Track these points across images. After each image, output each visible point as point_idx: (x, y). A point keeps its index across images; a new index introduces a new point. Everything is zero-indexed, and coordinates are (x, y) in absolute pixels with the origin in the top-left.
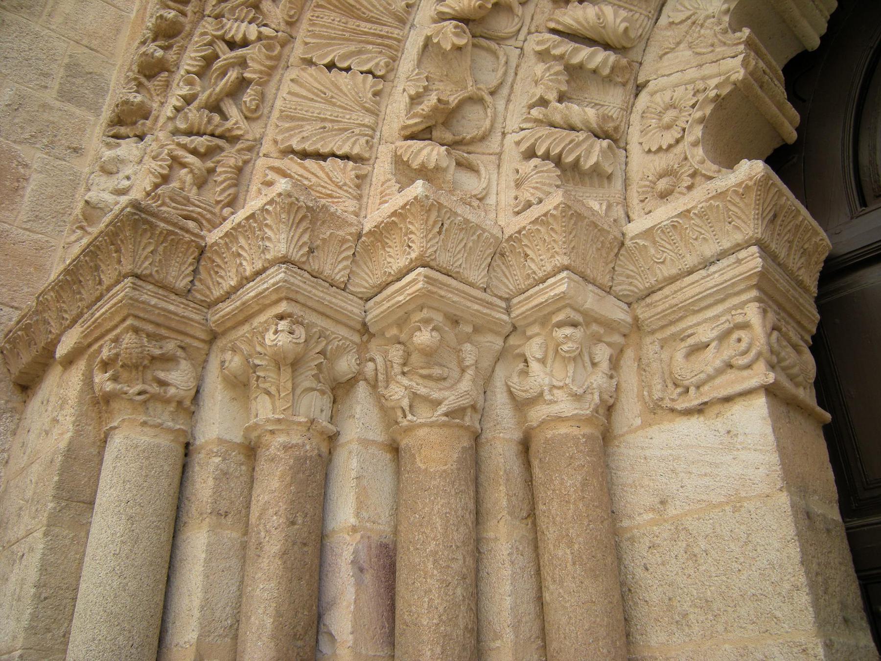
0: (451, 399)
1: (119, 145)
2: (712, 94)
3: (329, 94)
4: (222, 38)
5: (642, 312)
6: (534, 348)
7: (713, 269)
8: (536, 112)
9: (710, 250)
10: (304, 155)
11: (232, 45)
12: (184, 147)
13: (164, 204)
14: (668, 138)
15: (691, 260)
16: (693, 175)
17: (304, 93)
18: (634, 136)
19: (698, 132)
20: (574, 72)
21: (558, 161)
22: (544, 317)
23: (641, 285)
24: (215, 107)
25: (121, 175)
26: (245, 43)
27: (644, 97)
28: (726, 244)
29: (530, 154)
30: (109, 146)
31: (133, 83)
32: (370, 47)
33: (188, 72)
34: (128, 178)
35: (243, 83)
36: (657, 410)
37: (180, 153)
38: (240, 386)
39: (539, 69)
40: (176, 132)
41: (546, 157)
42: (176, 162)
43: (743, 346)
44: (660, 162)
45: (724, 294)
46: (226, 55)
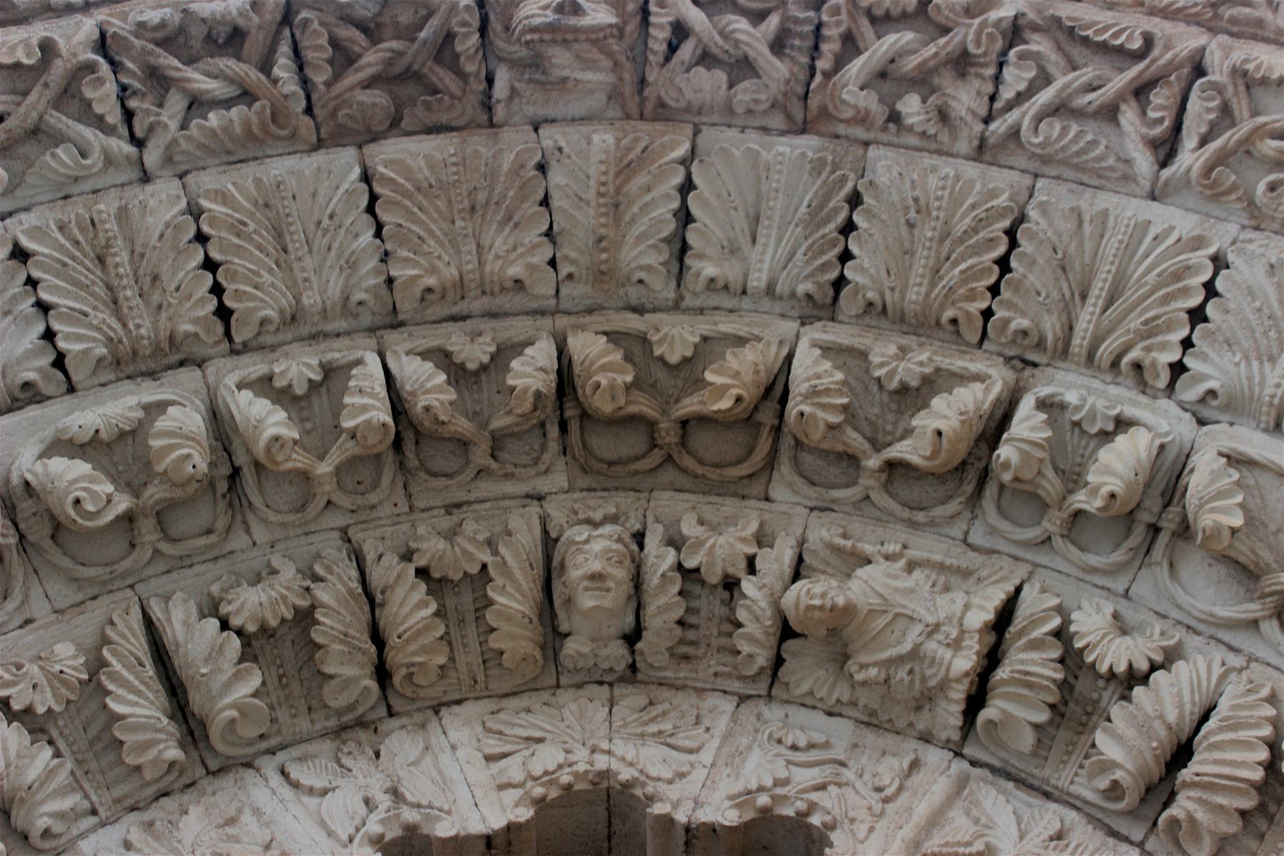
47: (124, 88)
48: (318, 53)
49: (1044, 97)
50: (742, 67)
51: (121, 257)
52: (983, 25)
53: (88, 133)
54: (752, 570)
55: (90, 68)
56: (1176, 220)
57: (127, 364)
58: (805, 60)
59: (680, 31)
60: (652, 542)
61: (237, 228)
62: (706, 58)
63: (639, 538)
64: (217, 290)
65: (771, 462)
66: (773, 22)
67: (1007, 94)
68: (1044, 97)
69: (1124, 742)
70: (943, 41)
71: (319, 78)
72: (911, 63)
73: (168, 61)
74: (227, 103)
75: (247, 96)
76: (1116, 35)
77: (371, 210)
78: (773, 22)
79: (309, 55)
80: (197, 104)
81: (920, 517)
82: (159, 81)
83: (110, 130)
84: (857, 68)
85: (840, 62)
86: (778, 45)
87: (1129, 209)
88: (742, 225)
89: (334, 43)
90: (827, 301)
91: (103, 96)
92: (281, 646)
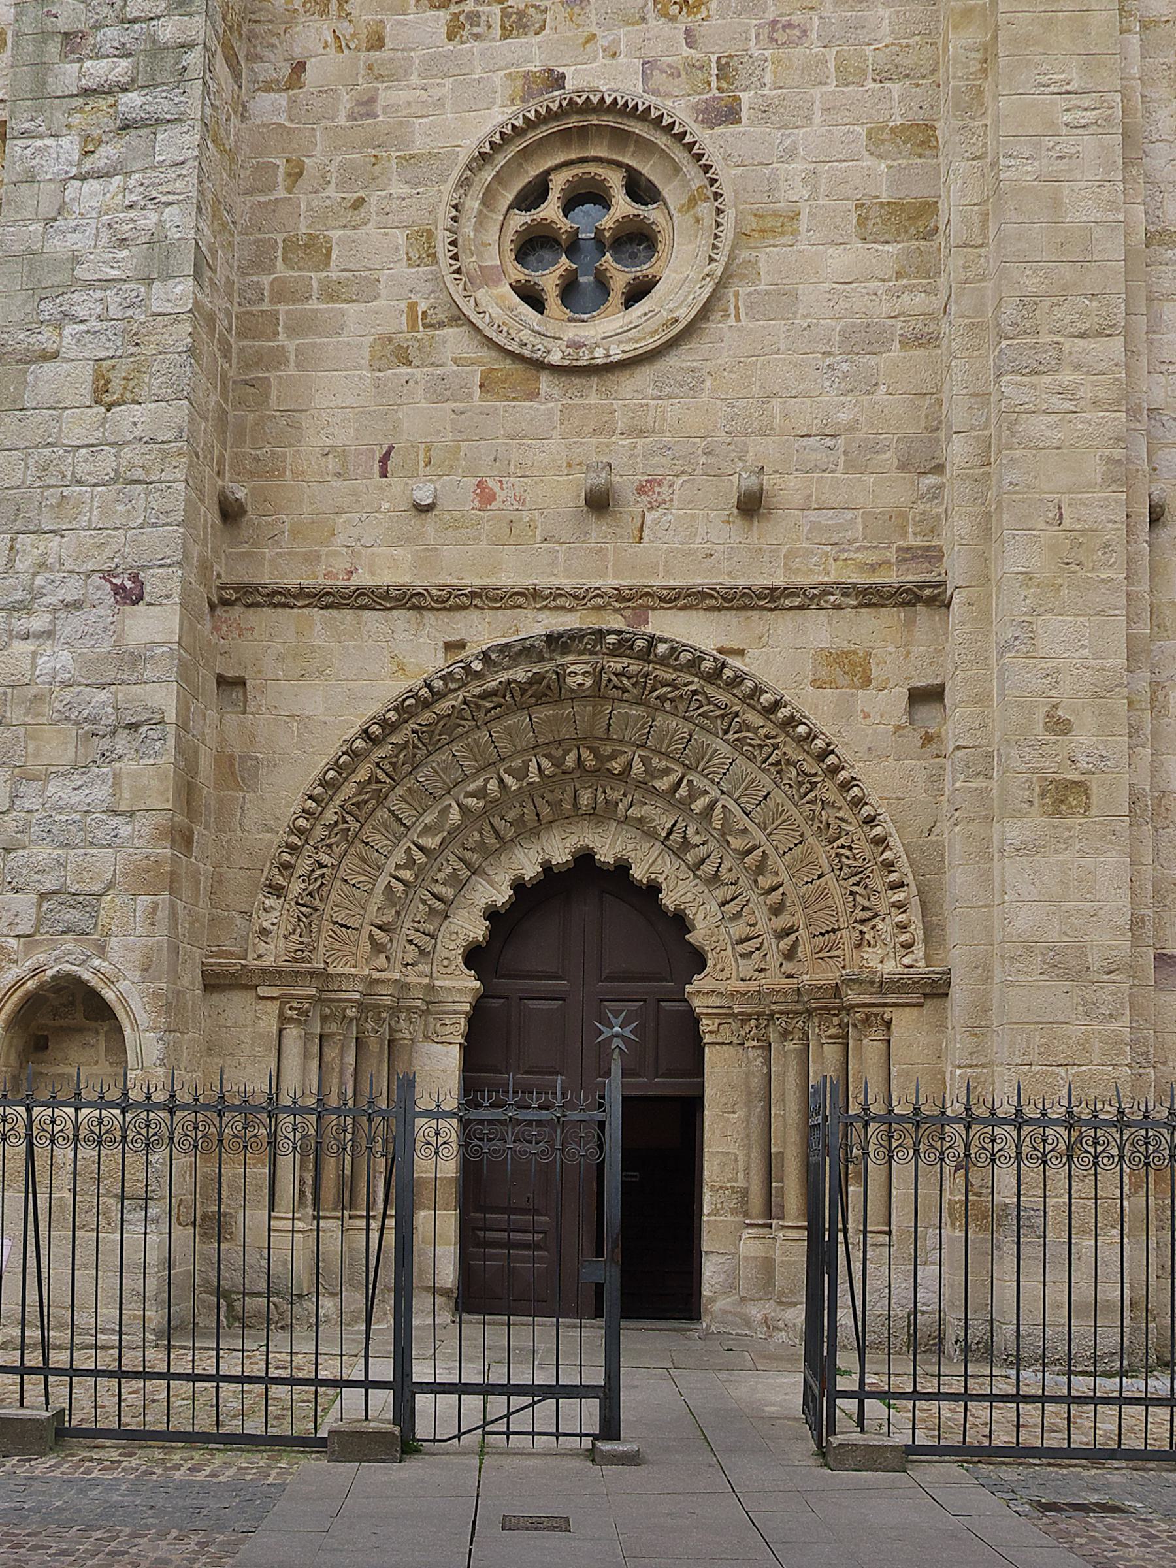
0: (382, 1030)
5: (432, 1007)
6: (403, 1016)
8: (416, 925)
10: (342, 925)
11: (321, 866)
18: (440, 938)
20: (432, 911)
22: (408, 1009)
23: (433, 999)
25: (271, 915)
27: (447, 922)
29: (410, 942)
35: (323, 884)
36: (426, 1037)
38: (324, 1019)
39: (421, 906)
40: (297, 903)
41: (416, 945)
42: (300, 920)
44: (446, 954)
46: (319, 872)
48: (517, 694)
49: (700, 711)
51: (475, 749)
53: (463, 722)
56: (725, 749)
57: (480, 770)
59: (610, 680)
61: (500, 737)
62: (615, 687)
68: (700, 711)
69: (690, 857)
72: (670, 696)
73: (481, 702)
74: (495, 708)
82: (478, 707)
85: (651, 692)
87: (717, 744)
90: (643, 746)
91: (468, 715)
92: (521, 820)
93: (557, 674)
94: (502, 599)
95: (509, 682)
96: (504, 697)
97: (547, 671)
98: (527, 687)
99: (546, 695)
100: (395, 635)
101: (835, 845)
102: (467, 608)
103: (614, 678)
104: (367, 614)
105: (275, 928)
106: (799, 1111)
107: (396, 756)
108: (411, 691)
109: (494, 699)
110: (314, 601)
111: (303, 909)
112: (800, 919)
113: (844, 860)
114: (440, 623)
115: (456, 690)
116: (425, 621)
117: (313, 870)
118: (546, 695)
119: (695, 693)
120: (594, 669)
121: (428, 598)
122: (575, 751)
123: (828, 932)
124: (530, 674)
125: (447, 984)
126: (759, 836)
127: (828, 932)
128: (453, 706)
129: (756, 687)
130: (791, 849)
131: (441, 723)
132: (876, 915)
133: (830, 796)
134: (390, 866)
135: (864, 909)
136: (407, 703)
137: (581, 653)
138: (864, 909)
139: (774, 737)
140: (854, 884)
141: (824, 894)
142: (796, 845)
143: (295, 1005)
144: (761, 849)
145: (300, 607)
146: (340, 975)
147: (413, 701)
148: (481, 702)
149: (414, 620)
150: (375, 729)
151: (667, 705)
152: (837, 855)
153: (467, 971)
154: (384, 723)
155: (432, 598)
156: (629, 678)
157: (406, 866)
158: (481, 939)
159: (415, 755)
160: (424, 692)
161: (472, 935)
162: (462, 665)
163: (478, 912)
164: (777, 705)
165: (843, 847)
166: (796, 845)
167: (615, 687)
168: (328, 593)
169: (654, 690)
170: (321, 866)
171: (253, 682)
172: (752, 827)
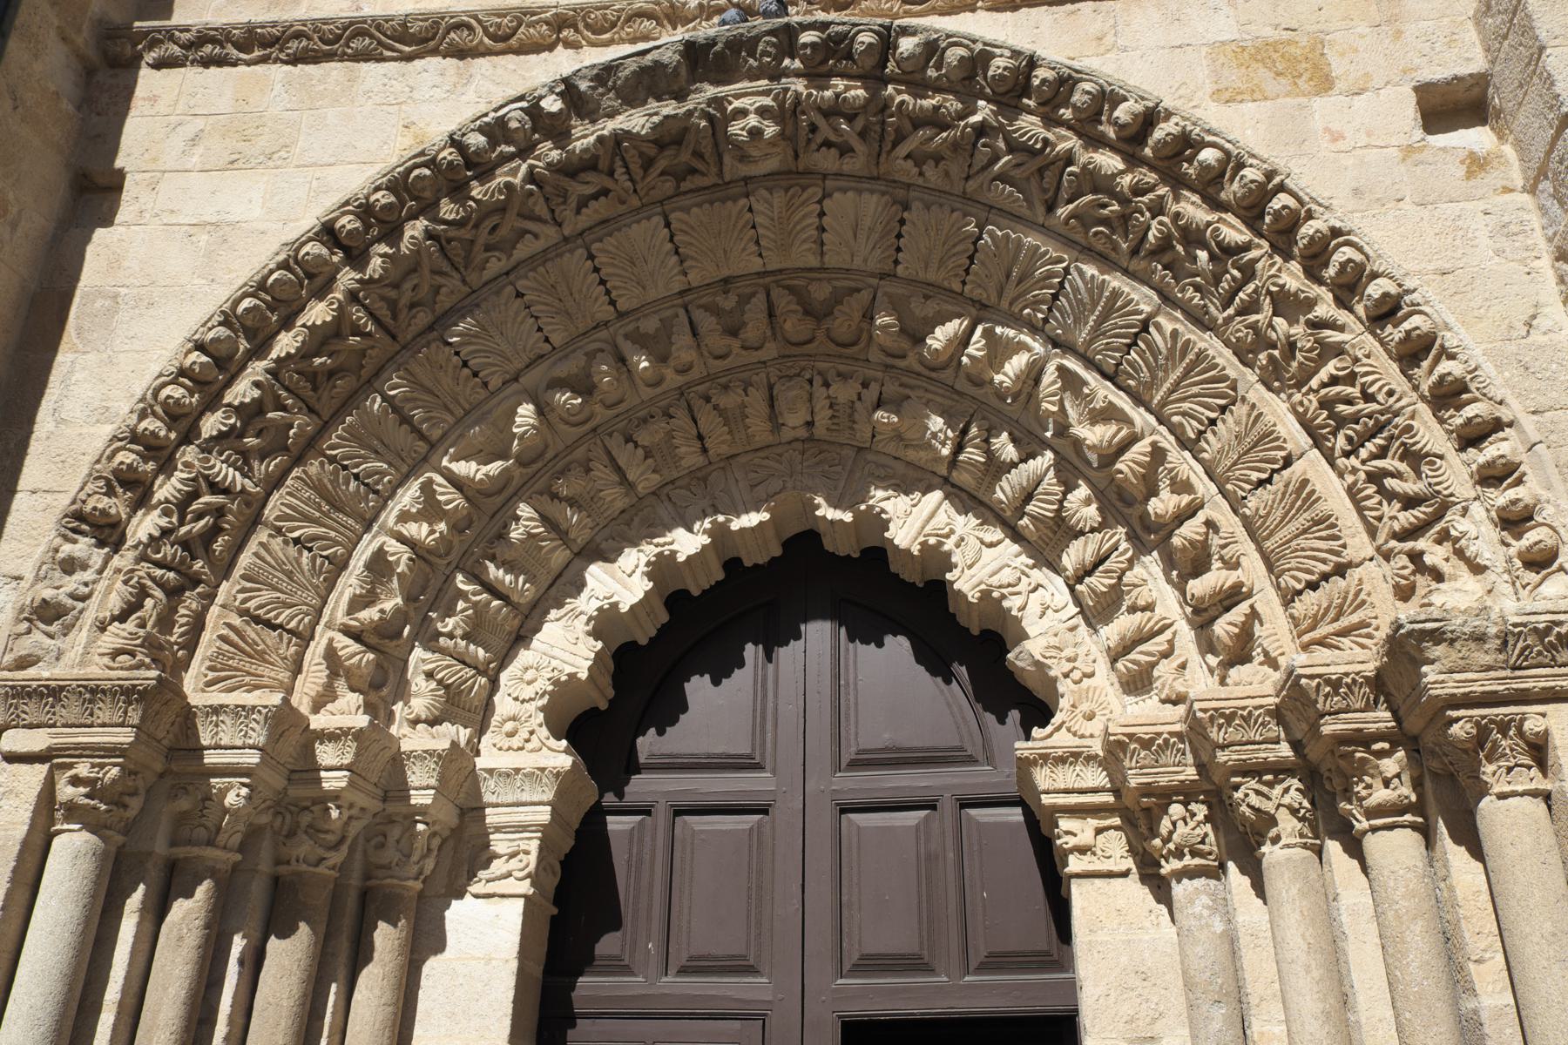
1: (75, 542)
2: (564, 678)
3: (289, 567)
4: (206, 477)
7: (521, 809)
9: (525, 797)
10: (257, 620)
11: (215, 488)
12: (153, 579)
13: (141, 646)
14: (528, 692)
15: (510, 799)
16: (532, 733)
17: (269, 559)
19: (545, 700)
21: (447, 687)
24: (185, 544)
26: (226, 491)
28: (536, 798)
30: (66, 539)
31: (102, 483)
32: (333, 534)
33: (167, 501)
34: (86, 584)
37: (149, 583)
43: (522, 865)
45: (522, 828)
47: (547, 200)
50: (845, 150)
52: (966, 126)
54: (860, 399)
55: (531, 193)
58: (876, 145)
59: (813, 128)
60: (818, 381)
62: (827, 144)
63: (811, 381)
64: (608, 292)
65: (868, 344)
66: (860, 123)
67: (976, 168)
70: (944, 135)
71: (638, 178)
74: (595, 197)
75: (605, 192)
76: (1030, 139)
77: (671, 240)
78: (860, 123)
79: (631, 166)
80: (583, 203)
81: (934, 375)
83: (545, 222)
84: (903, 150)
85: (895, 145)
86: (863, 135)
88: (850, 234)
89: (641, 154)
93: (710, 119)
94: (614, 25)
95: (619, 138)
96: (611, 173)
97: (690, 113)
98: (651, 150)
99: (693, 171)
100: (415, 95)
101: (1314, 383)
102: (551, 48)
103: (821, 122)
104: (365, 67)
105: (80, 605)
106: (1327, 1015)
107: (396, 286)
108: (422, 153)
109: (590, 176)
110: (274, 52)
111: (159, 572)
112: (1252, 570)
113: (1341, 408)
114: (499, 71)
115: (510, 158)
116: (473, 70)
117: (195, 495)
118: (693, 171)
119: (982, 129)
120: (781, 105)
121: (479, 30)
122: (761, 296)
123: (1325, 577)
124: (656, 119)
125: (505, 762)
126: (1141, 417)
127: (1325, 577)
128: (508, 185)
129: (1103, 92)
130: (1213, 422)
131: (488, 224)
132: (1444, 507)
133: (1292, 278)
134: (389, 517)
135: (1410, 502)
136: (416, 172)
137: (753, 77)
138: (1410, 502)
139: (1152, 189)
140: (1374, 457)
141: (1303, 494)
142: (1223, 409)
143: (83, 769)
144: (1147, 440)
145: (248, 63)
146: (217, 710)
147: (427, 172)
148: (566, 182)
149: (452, 71)
150: (348, 223)
151: (929, 169)
152: (1325, 404)
153: (552, 742)
154: (365, 211)
155: (485, 30)
156: (850, 119)
157: (416, 518)
158: (583, 675)
159: (437, 290)
160: (448, 154)
161: (569, 670)
162: (524, 104)
163: (581, 626)
164: (1150, 118)
165: (1334, 381)
166: (1223, 409)
167: (827, 144)
168: (298, 35)
169: (900, 138)
170: (215, 488)
171: (139, 177)
172: (1123, 402)
